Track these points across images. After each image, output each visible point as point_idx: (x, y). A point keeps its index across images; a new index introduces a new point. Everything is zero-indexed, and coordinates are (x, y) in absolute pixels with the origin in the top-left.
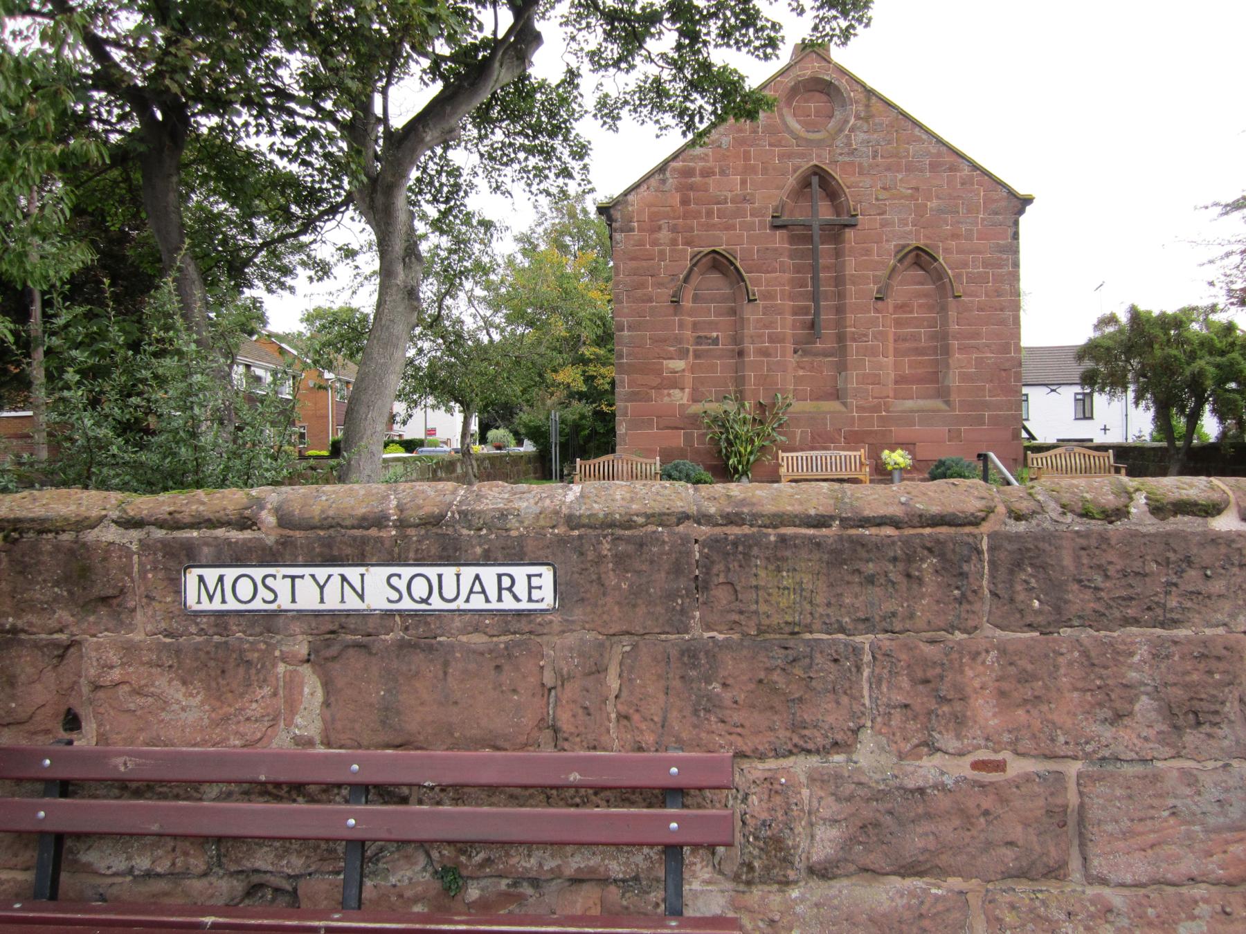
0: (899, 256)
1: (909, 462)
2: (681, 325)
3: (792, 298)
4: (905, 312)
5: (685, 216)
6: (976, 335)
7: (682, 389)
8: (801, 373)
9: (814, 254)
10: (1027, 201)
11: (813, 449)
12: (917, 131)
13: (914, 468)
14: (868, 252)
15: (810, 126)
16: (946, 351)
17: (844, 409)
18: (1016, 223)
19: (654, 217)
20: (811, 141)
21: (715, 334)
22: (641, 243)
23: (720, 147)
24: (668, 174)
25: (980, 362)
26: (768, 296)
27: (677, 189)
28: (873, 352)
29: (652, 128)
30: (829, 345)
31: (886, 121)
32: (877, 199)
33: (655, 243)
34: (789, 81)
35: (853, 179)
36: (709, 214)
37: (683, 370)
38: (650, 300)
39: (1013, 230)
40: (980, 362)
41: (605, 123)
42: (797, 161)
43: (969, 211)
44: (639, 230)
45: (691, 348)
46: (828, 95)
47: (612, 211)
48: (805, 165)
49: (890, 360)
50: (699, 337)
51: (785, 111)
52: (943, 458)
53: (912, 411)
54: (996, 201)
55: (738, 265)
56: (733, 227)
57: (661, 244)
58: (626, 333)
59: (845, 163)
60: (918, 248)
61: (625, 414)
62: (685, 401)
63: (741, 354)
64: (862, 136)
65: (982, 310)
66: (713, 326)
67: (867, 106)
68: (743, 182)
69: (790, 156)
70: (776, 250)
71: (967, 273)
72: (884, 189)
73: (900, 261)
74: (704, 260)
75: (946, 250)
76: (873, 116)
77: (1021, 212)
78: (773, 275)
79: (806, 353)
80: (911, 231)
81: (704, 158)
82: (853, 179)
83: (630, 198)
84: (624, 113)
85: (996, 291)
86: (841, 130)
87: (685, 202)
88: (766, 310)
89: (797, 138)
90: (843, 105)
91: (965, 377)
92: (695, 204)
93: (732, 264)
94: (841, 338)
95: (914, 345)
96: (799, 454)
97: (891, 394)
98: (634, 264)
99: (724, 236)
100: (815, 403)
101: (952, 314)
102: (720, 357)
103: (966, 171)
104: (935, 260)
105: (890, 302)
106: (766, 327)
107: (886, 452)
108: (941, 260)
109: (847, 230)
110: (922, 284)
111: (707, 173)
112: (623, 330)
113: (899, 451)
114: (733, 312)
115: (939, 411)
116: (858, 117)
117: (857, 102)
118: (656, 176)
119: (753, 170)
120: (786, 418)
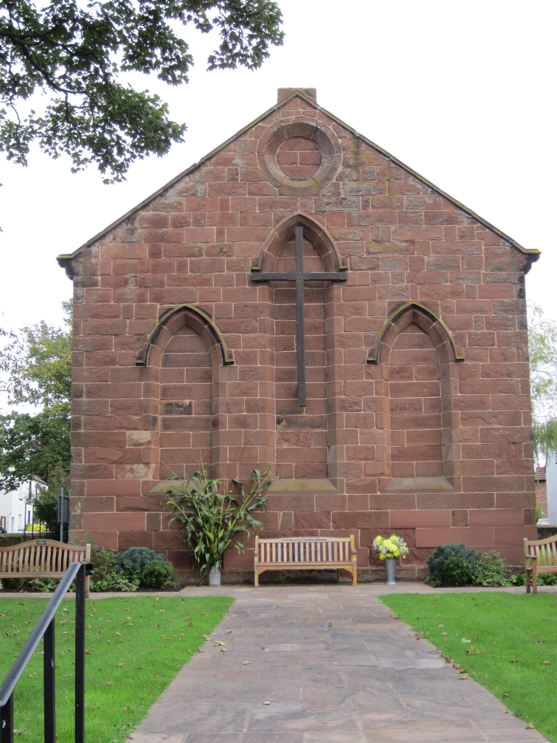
0: (393, 315)
1: (405, 549)
2: (148, 391)
3: (272, 360)
4: (403, 378)
5: (155, 269)
6: (482, 404)
7: (147, 464)
8: (285, 446)
9: (299, 313)
10: (533, 256)
11: (297, 534)
12: (411, 180)
13: (411, 557)
14: (358, 310)
15: (294, 174)
16: (449, 422)
17: (332, 488)
18: (522, 280)
19: (120, 270)
20: (295, 189)
21: (187, 402)
22: (104, 299)
23: (194, 195)
24: (137, 224)
25: (486, 434)
26: (247, 358)
27: (147, 240)
28: (366, 423)
29: (66, 160)
30: (319, 414)
31: (378, 169)
32: (368, 253)
33: (120, 299)
34: (271, 126)
35: (342, 231)
36: (182, 267)
37: (149, 442)
38: (113, 362)
39: (519, 287)
40: (486, 434)
41: (11, 155)
42: (280, 211)
43: (470, 266)
44: (105, 284)
45: (160, 417)
46: (314, 141)
47: (73, 264)
48: (288, 215)
49: (387, 431)
50: (169, 405)
51: (267, 158)
52: (444, 546)
53: (411, 491)
54: (498, 255)
55: (213, 324)
56: (207, 282)
57: (127, 300)
58: (84, 399)
59: (333, 213)
60: (414, 306)
61: (81, 493)
62: (150, 478)
63: (215, 424)
64: (351, 185)
65: (488, 375)
66: (185, 392)
67: (357, 153)
68: (220, 233)
69: (271, 205)
70: (255, 307)
71: (470, 334)
72: (376, 241)
73: (395, 320)
74: (175, 318)
75: (445, 309)
76: (362, 164)
77: (526, 269)
78: (253, 335)
79: (290, 423)
80: (405, 289)
81: (177, 207)
82: (342, 231)
83: (94, 249)
84: (34, 144)
85: (503, 354)
86: (328, 179)
87: (155, 254)
88: (244, 375)
89: (280, 186)
90: (331, 152)
91: (469, 452)
92: (167, 256)
93: (206, 322)
94: (329, 406)
95: (414, 415)
96: (279, 540)
97: (387, 471)
98: (94, 322)
99: (198, 291)
100: (301, 481)
101: (454, 380)
102: (192, 428)
103: (465, 223)
104: (434, 319)
105: (385, 366)
106: (243, 393)
107: (379, 538)
108: (440, 320)
109: (335, 286)
110: (422, 347)
111: (179, 223)
112: (81, 396)
113: (394, 538)
114: (208, 376)
115: (441, 490)
116: (346, 165)
117: (344, 149)
118: (124, 225)
119: (231, 220)
120: (264, 500)
